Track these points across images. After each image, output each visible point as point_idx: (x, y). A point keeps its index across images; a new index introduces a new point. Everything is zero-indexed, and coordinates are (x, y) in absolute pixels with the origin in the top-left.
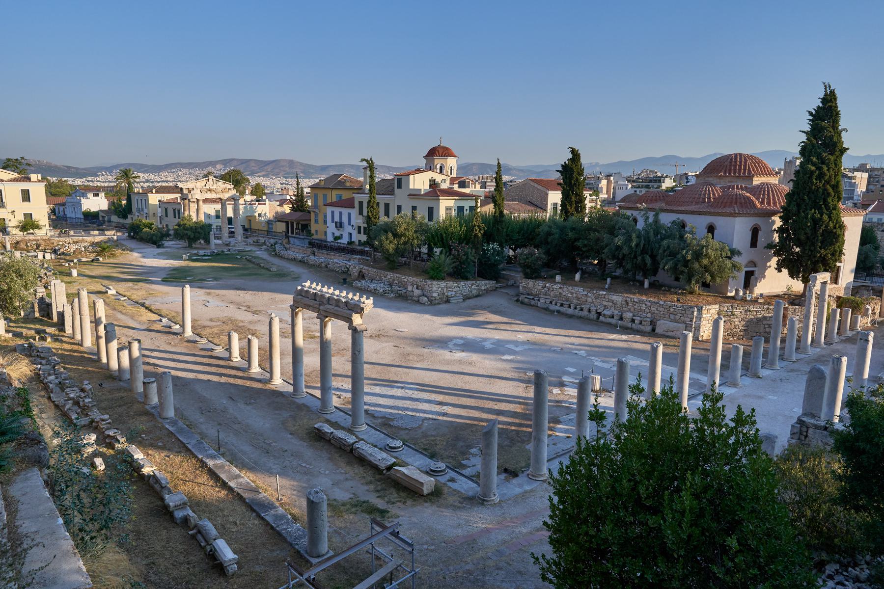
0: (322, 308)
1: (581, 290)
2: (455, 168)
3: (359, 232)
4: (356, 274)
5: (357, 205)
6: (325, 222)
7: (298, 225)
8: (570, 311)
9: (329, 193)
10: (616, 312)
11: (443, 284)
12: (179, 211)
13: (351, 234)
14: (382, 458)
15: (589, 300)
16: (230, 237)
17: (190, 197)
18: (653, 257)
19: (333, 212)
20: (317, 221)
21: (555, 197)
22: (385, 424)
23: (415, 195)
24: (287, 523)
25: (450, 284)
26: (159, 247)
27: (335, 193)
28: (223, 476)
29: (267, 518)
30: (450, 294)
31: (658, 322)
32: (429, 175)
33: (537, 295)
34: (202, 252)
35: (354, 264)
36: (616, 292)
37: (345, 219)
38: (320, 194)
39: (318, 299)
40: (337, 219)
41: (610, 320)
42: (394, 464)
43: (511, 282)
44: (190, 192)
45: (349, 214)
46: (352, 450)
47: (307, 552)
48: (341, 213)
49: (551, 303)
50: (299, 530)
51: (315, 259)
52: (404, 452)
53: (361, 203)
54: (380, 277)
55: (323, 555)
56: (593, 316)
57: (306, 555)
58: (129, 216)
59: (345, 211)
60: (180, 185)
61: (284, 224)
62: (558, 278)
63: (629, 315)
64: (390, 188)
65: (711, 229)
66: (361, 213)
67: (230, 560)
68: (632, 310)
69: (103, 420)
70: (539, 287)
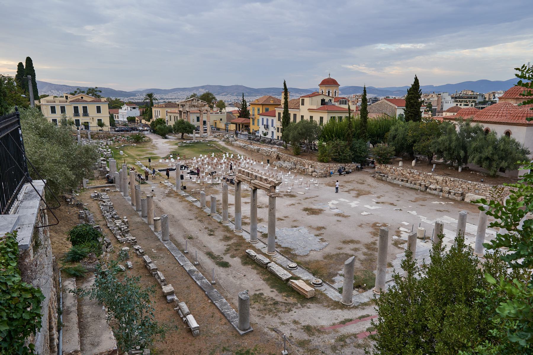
0: (252, 181)
1: (415, 171)
3: (278, 131)
4: (275, 157)
6: (258, 125)
7: (243, 125)
8: (408, 185)
10: (438, 187)
11: (327, 165)
12: (177, 117)
13: (273, 132)
14: (284, 274)
15: (421, 178)
16: (204, 133)
18: (466, 152)
19: (263, 119)
20: (253, 124)
22: (287, 252)
24: (228, 309)
25: (331, 165)
26: (166, 138)
28: (193, 277)
29: (216, 304)
30: (331, 171)
31: (467, 195)
33: (386, 174)
35: (274, 150)
36: (439, 175)
38: (256, 108)
39: (250, 176)
40: (265, 123)
41: (434, 192)
42: (291, 278)
45: (272, 120)
46: (267, 267)
47: (237, 327)
48: (267, 120)
50: (234, 313)
51: (252, 147)
52: (297, 270)
54: (289, 159)
55: (247, 330)
56: (423, 188)
57: (237, 329)
58: (151, 120)
59: (270, 119)
62: (401, 164)
63: (447, 189)
64: (297, 105)
65: (508, 133)
66: (279, 120)
67: (195, 328)
68: (449, 186)
69: (132, 240)
70: (388, 169)
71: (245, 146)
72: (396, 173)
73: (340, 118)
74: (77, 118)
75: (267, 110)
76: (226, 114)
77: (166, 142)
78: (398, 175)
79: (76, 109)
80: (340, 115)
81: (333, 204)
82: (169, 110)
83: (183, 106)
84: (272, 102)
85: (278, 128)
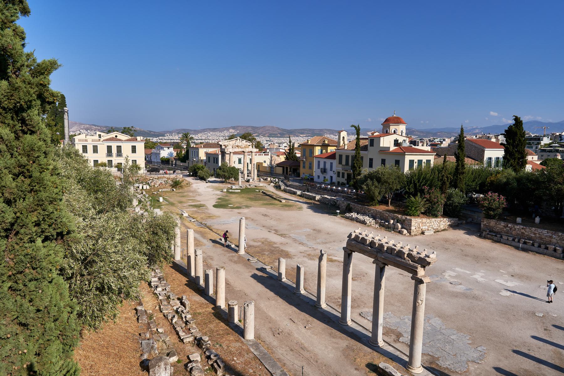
2: (404, 131)
3: (338, 176)
5: (337, 157)
7: (290, 169)
13: (332, 177)
17: (226, 151)
19: (319, 162)
20: (304, 167)
21: (495, 154)
23: (386, 150)
32: (394, 137)
43: (470, 220)
44: (226, 147)
45: (331, 164)
48: (325, 163)
49: (514, 240)
58: (187, 161)
60: (220, 143)
66: (340, 162)
72: (514, 233)
73: (428, 161)
74: (110, 159)
78: (518, 235)
79: (109, 149)
80: (420, 158)
81: (450, 276)
85: (339, 173)
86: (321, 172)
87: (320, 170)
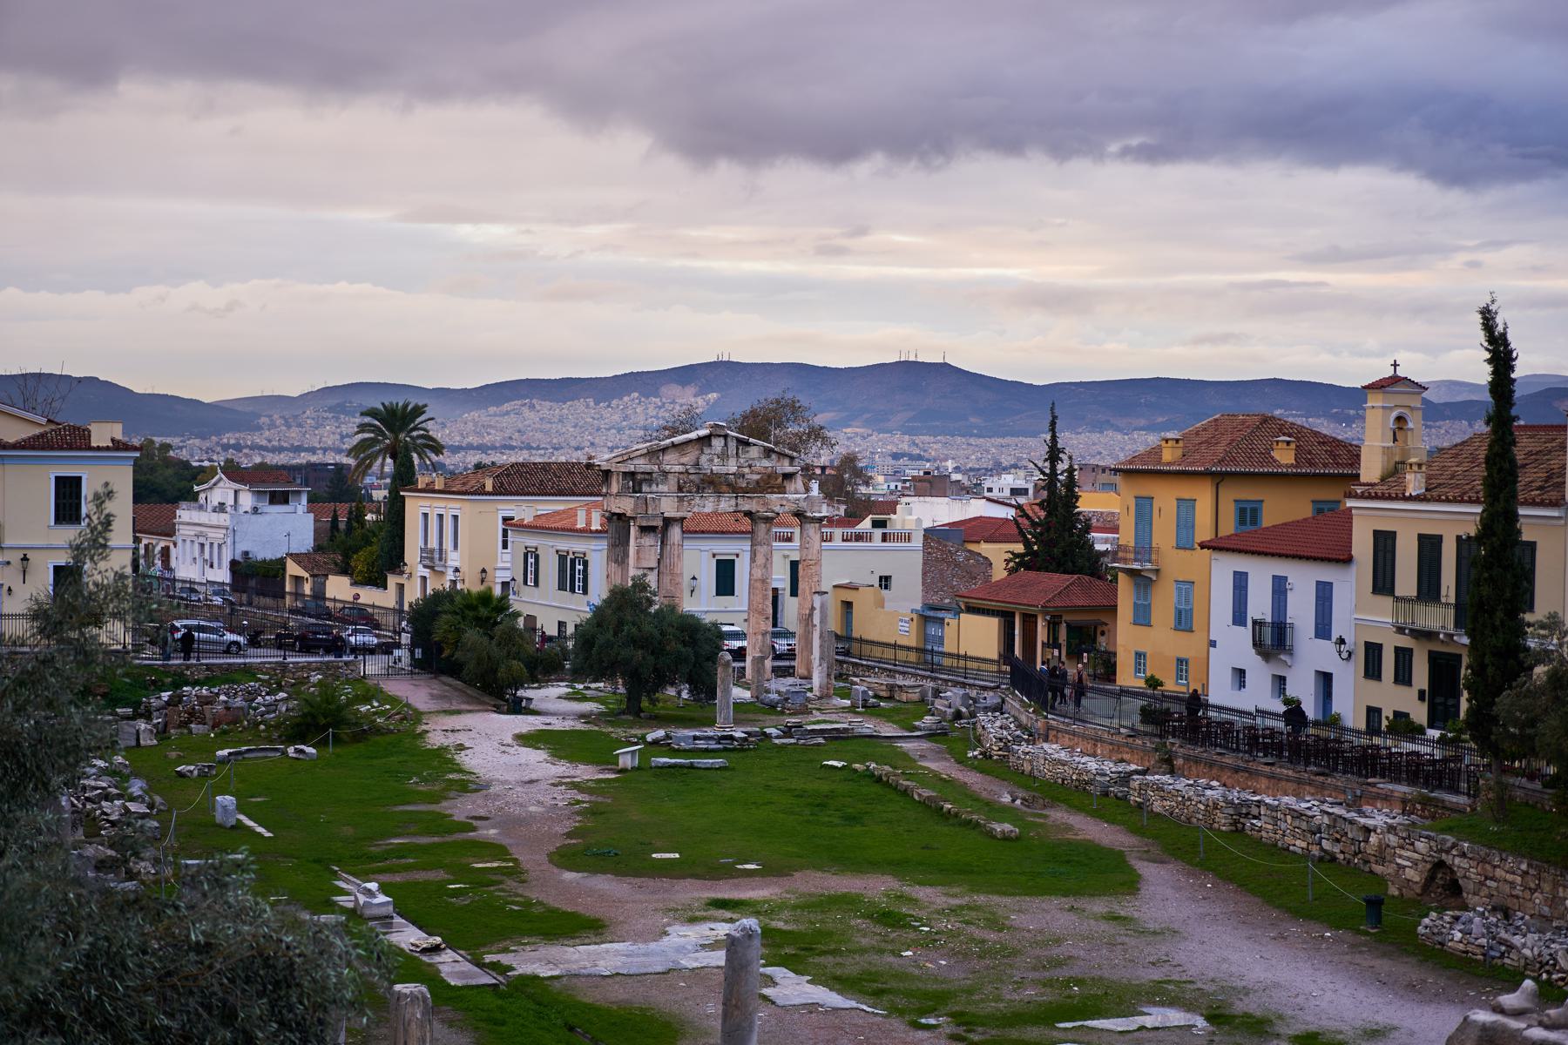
3: (1372, 670)
5: (1362, 546)
6: (1183, 621)
7: (1053, 626)
9: (1203, 497)
13: (1325, 679)
16: (780, 672)
19: (1240, 581)
20: (1142, 617)
26: (518, 707)
27: (1231, 495)
34: (684, 735)
37: (1301, 611)
40: (1260, 605)
45: (1324, 593)
48: (1280, 588)
53: (1384, 543)
58: (392, 581)
59: (1303, 580)
61: (992, 625)
66: (1383, 582)
71: (1125, 779)
75: (1248, 514)
76: (918, 542)
77: (526, 740)
82: (525, 509)
83: (635, 481)
84: (1285, 457)
85: (1373, 652)
86: (1257, 644)
87: (1246, 633)
